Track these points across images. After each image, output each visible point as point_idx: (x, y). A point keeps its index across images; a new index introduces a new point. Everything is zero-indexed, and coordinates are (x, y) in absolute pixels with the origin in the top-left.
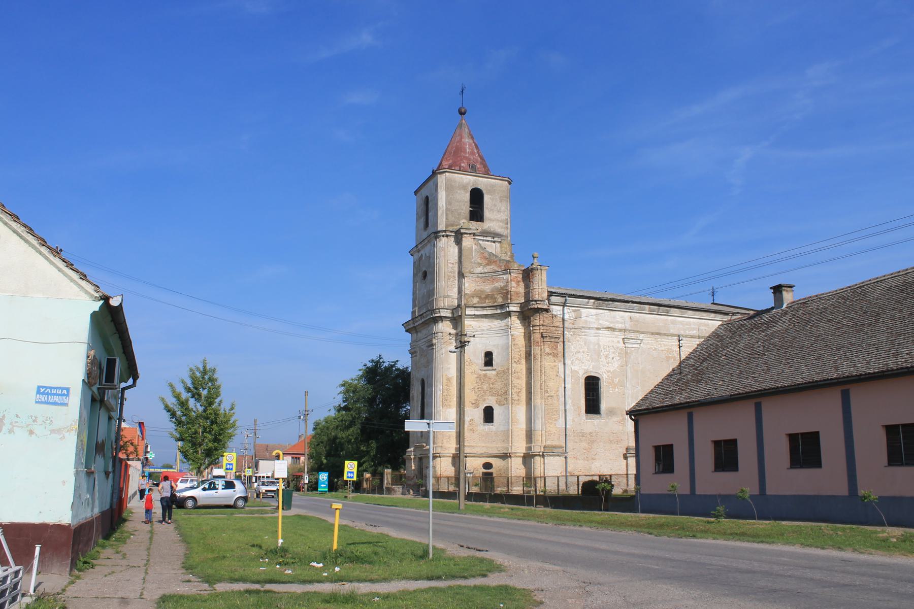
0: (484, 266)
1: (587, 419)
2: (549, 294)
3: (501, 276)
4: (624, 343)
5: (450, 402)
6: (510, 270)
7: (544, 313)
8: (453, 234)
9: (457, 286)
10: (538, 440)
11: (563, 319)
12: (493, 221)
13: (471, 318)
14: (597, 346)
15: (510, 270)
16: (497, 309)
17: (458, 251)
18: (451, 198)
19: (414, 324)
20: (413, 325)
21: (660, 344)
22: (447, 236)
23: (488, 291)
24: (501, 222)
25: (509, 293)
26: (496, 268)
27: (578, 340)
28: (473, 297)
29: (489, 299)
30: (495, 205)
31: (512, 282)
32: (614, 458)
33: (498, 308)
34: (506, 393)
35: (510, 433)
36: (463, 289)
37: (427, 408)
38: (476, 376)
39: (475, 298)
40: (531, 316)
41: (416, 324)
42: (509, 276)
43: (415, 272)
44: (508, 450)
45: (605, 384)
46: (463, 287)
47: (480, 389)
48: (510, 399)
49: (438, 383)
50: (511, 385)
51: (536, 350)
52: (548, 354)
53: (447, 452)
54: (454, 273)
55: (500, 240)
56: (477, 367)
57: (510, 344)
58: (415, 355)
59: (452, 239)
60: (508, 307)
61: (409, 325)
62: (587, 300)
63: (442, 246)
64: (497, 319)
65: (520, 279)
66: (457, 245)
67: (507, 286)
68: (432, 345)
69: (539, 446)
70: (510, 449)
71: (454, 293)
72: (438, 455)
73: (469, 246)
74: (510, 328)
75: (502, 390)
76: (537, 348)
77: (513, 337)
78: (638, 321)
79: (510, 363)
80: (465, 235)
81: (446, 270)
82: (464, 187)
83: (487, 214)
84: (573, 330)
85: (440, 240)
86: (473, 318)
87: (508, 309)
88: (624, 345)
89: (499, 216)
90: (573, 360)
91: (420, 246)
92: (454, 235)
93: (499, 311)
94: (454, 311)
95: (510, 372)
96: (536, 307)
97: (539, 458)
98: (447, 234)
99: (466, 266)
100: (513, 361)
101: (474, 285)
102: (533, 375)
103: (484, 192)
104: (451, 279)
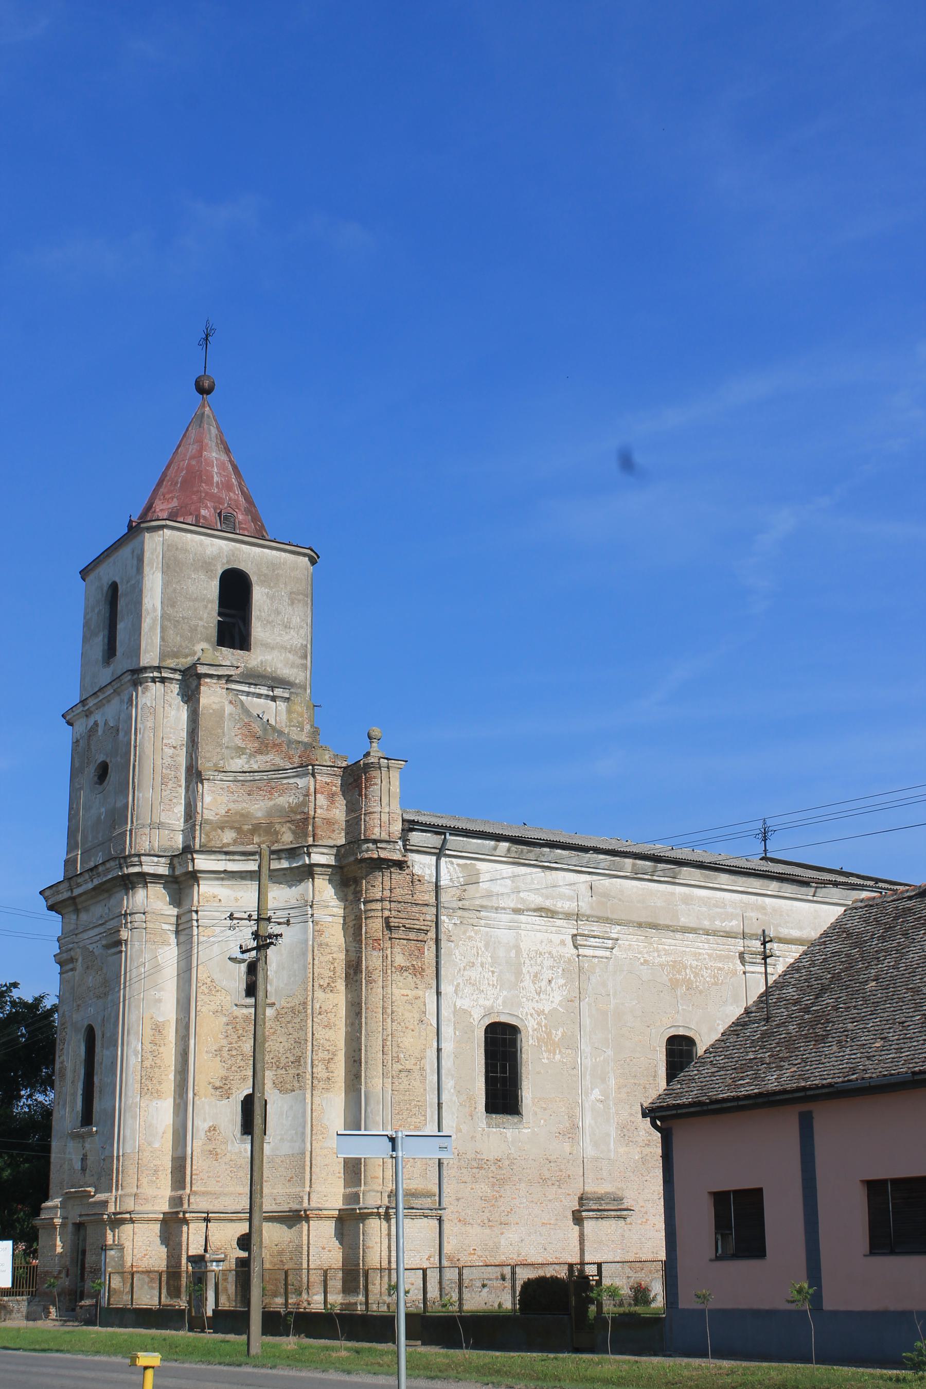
0: (250, 756)
1: (489, 1126)
2: (407, 825)
3: (291, 781)
4: (576, 947)
5: (160, 1083)
6: (313, 766)
7: (392, 870)
8: (178, 676)
9: (183, 802)
10: (377, 1178)
11: (437, 887)
12: (273, 648)
13: (217, 879)
14: (514, 951)
15: (313, 766)
16: (280, 859)
17: (188, 717)
18: (175, 590)
21: (658, 950)
22: (163, 680)
23: (259, 814)
24: (290, 652)
25: (311, 821)
26: (280, 762)
27: (470, 938)
28: (222, 829)
29: (260, 835)
30: (278, 613)
31: (318, 796)
32: (552, 1222)
33: (284, 856)
35: (308, 1159)
36: (199, 810)
37: (100, 1099)
38: (225, 1020)
39: (226, 830)
40: (362, 878)
41: (77, 892)
42: (312, 779)
43: (77, 765)
44: (301, 1202)
45: (531, 1042)
46: (199, 804)
47: (234, 1053)
48: (309, 1077)
49: (132, 1037)
50: (309, 1044)
51: (372, 960)
52: (402, 969)
53: (148, 1207)
54: (177, 769)
55: (287, 695)
56: (228, 998)
57: (311, 943)
58: (71, 966)
59: (175, 688)
60: (309, 854)
61: (58, 893)
62: (493, 843)
63: (149, 705)
64: (281, 883)
65: (336, 789)
66: (186, 702)
67: (305, 804)
68: (119, 943)
69: (378, 1192)
70: (306, 1201)
71: (176, 816)
72: (128, 1216)
73: (215, 706)
74: (311, 907)
75: (288, 1055)
76: (375, 953)
77: (317, 928)
78: (606, 895)
79: (310, 988)
80: (208, 680)
81: (159, 762)
82: (206, 566)
83: (258, 631)
84: (460, 913)
85: (146, 689)
86: (222, 879)
87: (307, 858)
88: (575, 951)
89: (287, 638)
90: (458, 984)
91: (91, 703)
92: (180, 677)
93: (285, 864)
94: (176, 861)
95: (309, 1011)
96: (376, 856)
97: (378, 1221)
98: (164, 675)
99: (208, 755)
100: (316, 984)
101: (225, 799)
102: (363, 1020)
103: (254, 579)
104: (170, 785)
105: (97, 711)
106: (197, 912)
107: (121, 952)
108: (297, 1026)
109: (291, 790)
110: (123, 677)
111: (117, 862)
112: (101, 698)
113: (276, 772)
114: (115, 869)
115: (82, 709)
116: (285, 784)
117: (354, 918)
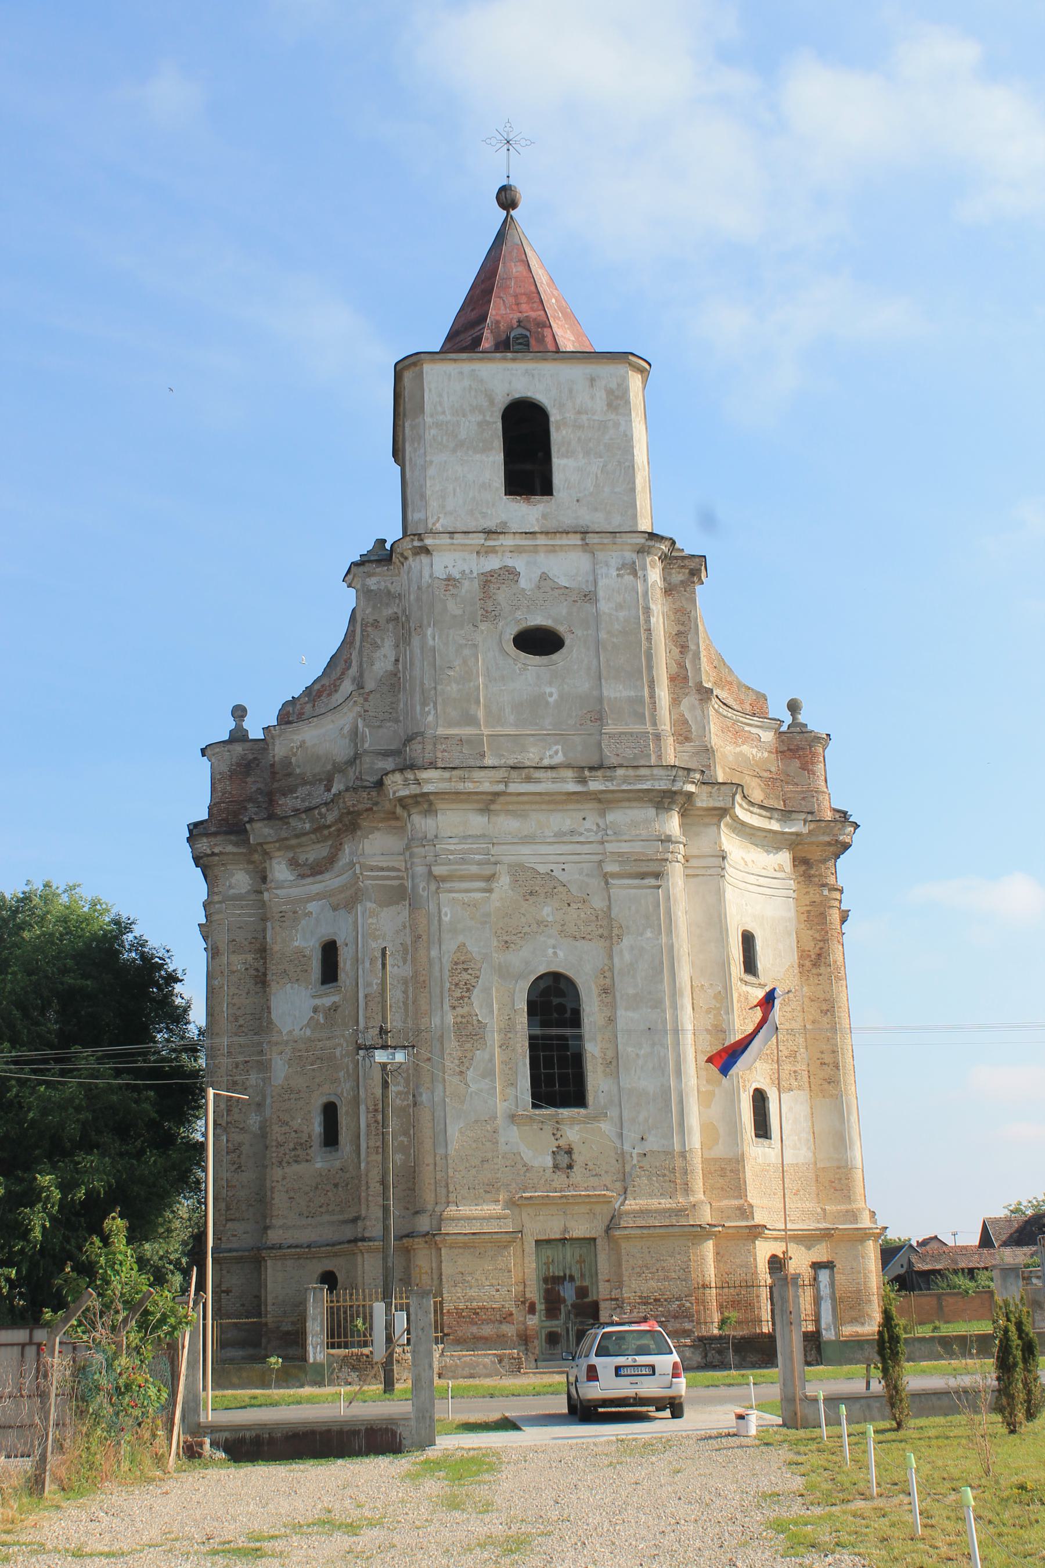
3: (754, 730)
19: (506, 784)
20: (501, 787)
34: (795, 1057)
41: (513, 788)
58: (482, 885)
61: (463, 779)
64: (756, 845)
68: (657, 875)
91: (508, 541)
93: (775, 826)
106: (724, 858)
107: (659, 887)
108: (789, 1015)
109: (752, 740)
110: (624, 535)
111: (674, 773)
112: (538, 542)
113: (744, 715)
114: (662, 779)
116: (746, 731)
117: (808, 903)
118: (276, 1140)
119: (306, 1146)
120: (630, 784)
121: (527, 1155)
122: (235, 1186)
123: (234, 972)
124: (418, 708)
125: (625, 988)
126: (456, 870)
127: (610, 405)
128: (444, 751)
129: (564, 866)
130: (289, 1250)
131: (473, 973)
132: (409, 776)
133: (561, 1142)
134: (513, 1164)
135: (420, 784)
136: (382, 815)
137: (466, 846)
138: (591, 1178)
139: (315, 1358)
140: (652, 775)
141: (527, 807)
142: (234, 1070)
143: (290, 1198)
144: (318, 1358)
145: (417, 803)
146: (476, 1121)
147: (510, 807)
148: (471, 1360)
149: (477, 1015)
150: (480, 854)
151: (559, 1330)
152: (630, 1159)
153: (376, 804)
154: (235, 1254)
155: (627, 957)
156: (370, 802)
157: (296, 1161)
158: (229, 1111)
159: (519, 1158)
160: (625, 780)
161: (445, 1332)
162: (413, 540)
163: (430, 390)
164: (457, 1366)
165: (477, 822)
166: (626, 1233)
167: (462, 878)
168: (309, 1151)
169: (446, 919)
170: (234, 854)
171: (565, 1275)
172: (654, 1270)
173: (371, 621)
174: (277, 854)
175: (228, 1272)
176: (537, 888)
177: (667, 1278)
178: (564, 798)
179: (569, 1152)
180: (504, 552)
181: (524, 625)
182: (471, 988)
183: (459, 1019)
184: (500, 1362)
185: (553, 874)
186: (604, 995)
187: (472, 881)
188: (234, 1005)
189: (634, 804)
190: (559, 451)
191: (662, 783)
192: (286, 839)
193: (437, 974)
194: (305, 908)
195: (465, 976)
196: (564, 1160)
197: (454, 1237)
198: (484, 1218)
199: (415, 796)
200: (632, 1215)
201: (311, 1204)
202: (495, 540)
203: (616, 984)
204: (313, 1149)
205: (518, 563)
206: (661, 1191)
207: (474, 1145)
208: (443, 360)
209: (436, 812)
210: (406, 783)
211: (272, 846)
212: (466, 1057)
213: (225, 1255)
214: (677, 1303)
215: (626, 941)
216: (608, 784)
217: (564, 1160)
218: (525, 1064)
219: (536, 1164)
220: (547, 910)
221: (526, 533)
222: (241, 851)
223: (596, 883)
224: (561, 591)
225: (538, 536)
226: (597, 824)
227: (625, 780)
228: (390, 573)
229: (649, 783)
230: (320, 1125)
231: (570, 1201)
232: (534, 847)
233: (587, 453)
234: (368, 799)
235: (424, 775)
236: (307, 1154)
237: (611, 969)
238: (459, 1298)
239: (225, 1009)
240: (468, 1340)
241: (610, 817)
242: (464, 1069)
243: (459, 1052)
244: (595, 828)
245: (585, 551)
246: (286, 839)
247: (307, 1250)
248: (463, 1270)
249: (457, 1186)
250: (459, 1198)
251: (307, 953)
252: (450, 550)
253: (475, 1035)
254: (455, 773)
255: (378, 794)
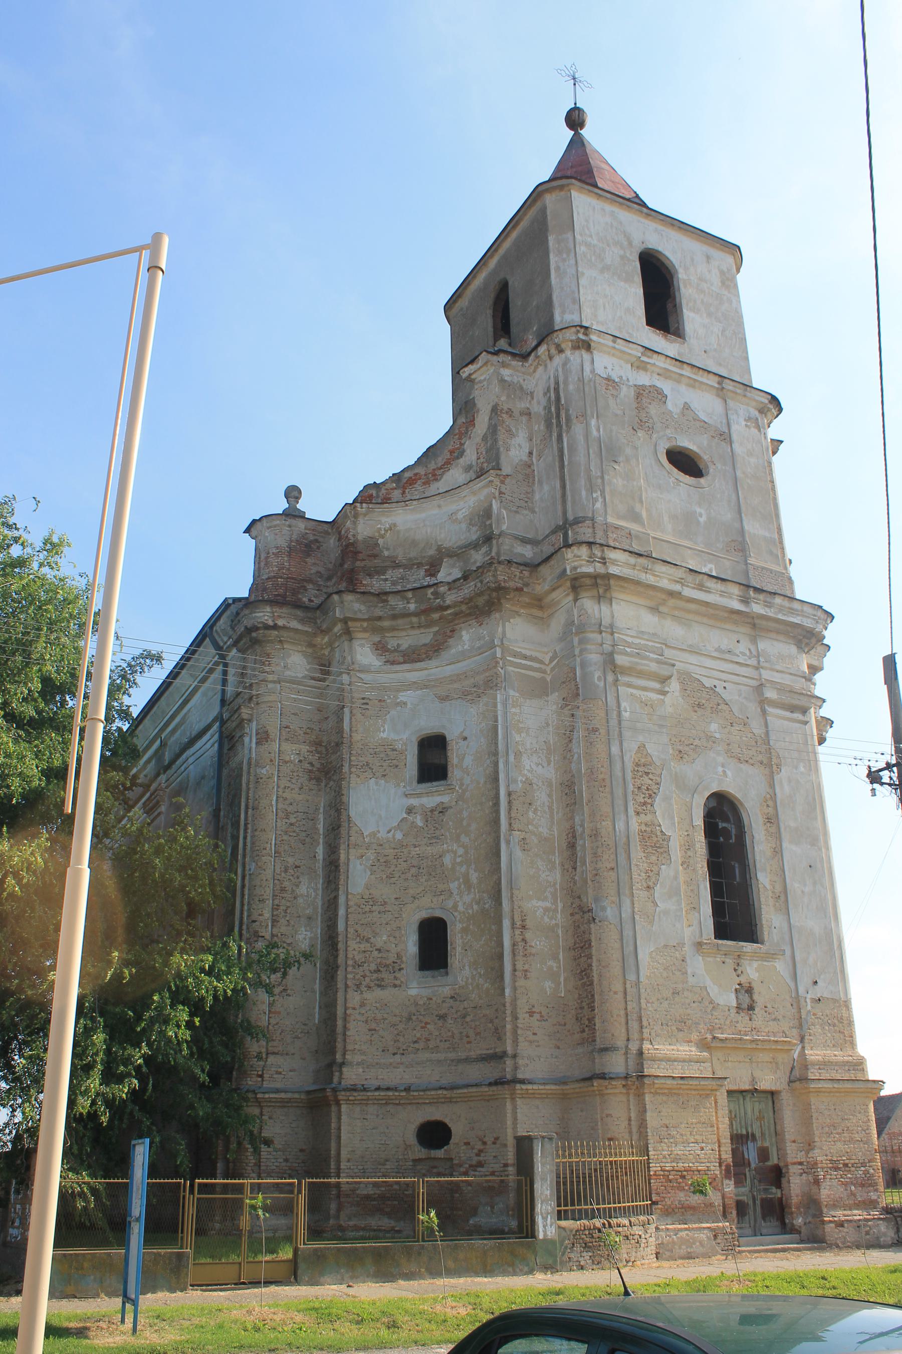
20: (677, 587)
58: (657, 685)
61: (645, 570)
91: (660, 362)
105: (657, 377)
112: (684, 373)
114: (809, 617)
115: (640, 355)
118: (353, 958)
119: (396, 967)
120: (785, 615)
121: (714, 991)
122: (279, 1013)
123: (286, 762)
124: (584, 493)
125: (788, 820)
126: (637, 663)
127: (723, 283)
128: (615, 540)
129: (725, 684)
130: (377, 1093)
131: (654, 778)
132: (596, 552)
133: (743, 979)
134: (700, 999)
135: (605, 563)
136: (527, 600)
137: (643, 642)
138: (771, 1023)
139: (545, 1232)
140: (802, 611)
141: (691, 616)
142: (283, 874)
143: (370, 1030)
144: (549, 1233)
145: (596, 585)
146: (666, 946)
147: (676, 613)
148: (687, 1235)
149: (660, 826)
150: (654, 653)
151: (744, 1198)
152: (804, 1004)
153: (527, 585)
154: (283, 1095)
155: (787, 788)
156: (520, 581)
157: (379, 986)
158: (275, 922)
159: (705, 993)
160: (781, 609)
161: (654, 1199)
162: (578, 332)
163: (578, 213)
164: (673, 1242)
165: (649, 621)
166: (820, 1086)
167: (641, 674)
168: (398, 975)
169: (626, 715)
170: (296, 631)
171: (748, 1133)
172: (840, 1131)
173: (505, 409)
174: (360, 635)
175: (270, 1118)
176: (704, 702)
177: (852, 1140)
178: (726, 615)
179: (749, 991)
180: (653, 372)
181: (674, 444)
182: (653, 795)
183: (643, 828)
184: (715, 1236)
185: (716, 689)
186: (768, 824)
187: (649, 679)
188: (286, 799)
189: (781, 637)
190: (687, 305)
191: (809, 621)
192: (380, 618)
193: (620, 774)
194: (396, 697)
195: (646, 780)
196: (746, 1000)
197: (663, 1081)
198: (684, 1061)
199: (595, 577)
200: (818, 1067)
201: (402, 1039)
202: (649, 357)
203: (780, 813)
204: (404, 972)
205: (666, 386)
206: (833, 1042)
207: (665, 974)
208: (590, 191)
209: (611, 600)
210: (591, 560)
211: (358, 624)
212: (652, 871)
213: (272, 1095)
214: (863, 1169)
215: (785, 772)
216: (768, 610)
217: (746, 1000)
218: (706, 887)
219: (721, 1002)
220: (714, 727)
221: (676, 360)
222: (306, 629)
223: (753, 708)
224: (702, 424)
225: (685, 366)
226: (749, 650)
227: (781, 609)
228: (523, 370)
229: (799, 618)
230: (415, 945)
231: (759, 1047)
232: (703, 659)
233: (710, 315)
234: (520, 578)
235: (612, 555)
236: (395, 978)
237: (774, 797)
238: (665, 1157)
239: (274, 803)
240: (676, 1210)
241: (762, 645)
242: (651, 884)
243: (645, 865)
244: (748, 653)
245: (718, 395)
246: (380, 618)
247: (404, 1094)
248: (667, 1122)
249: (650, 1021)
250: (653, 1034)
251: (399, 746)
252: (609, 353)
253: (659, 847)
254: (641, 560)
255: (530, 574)
